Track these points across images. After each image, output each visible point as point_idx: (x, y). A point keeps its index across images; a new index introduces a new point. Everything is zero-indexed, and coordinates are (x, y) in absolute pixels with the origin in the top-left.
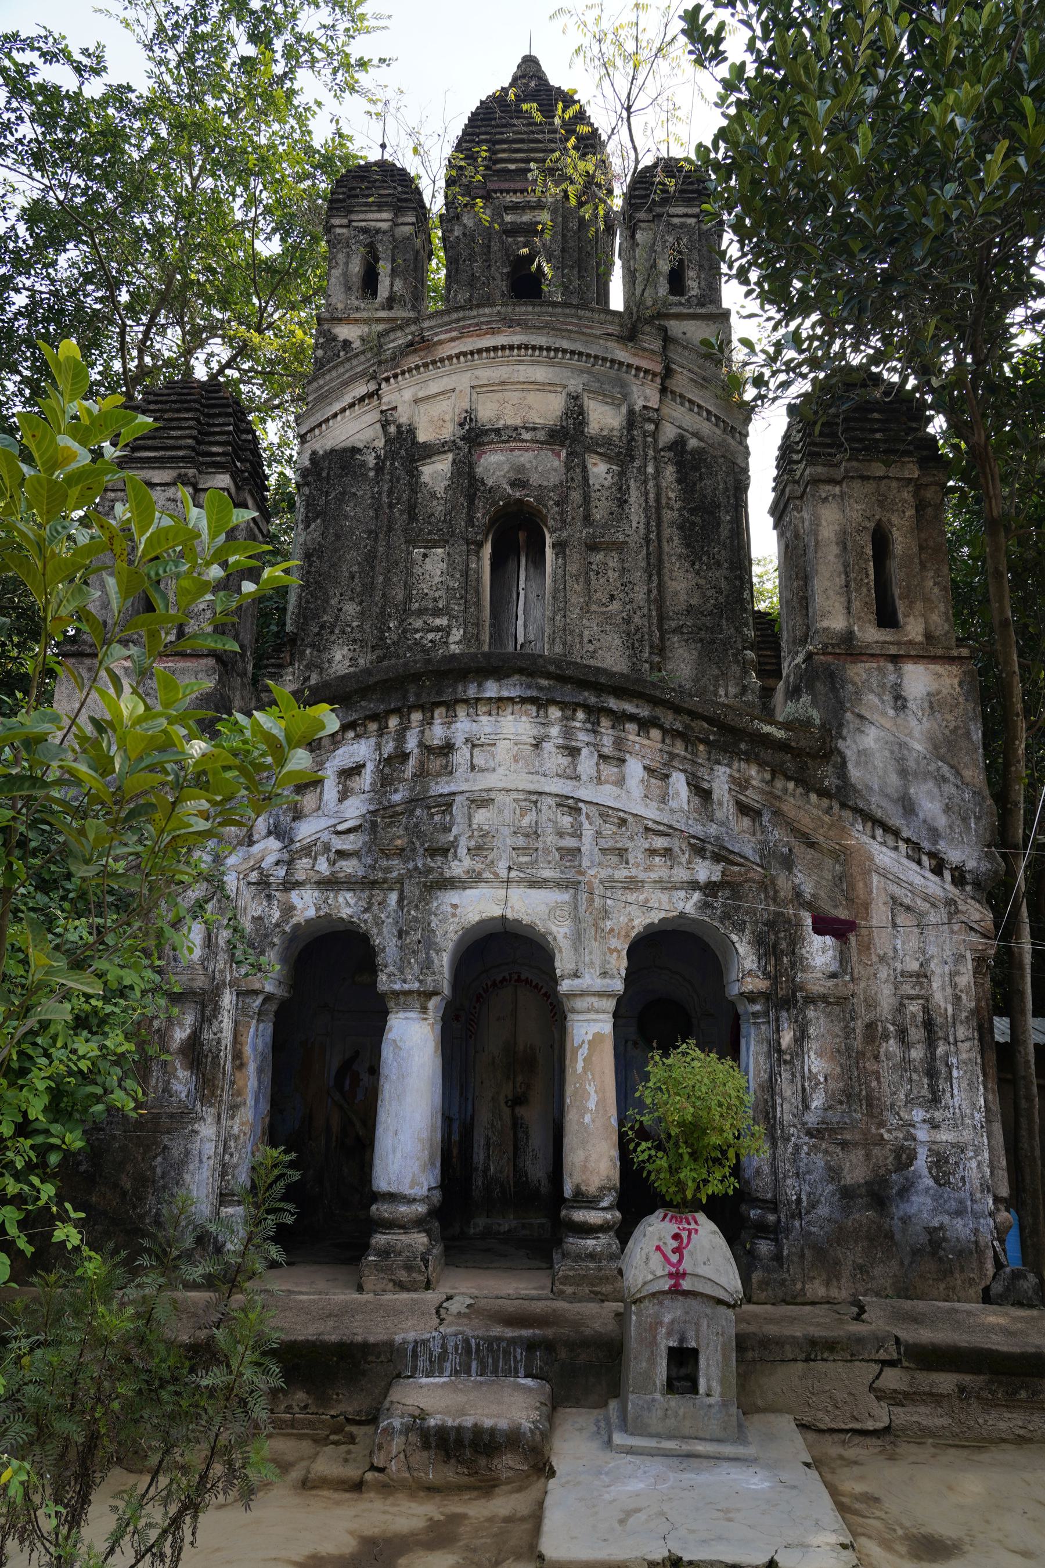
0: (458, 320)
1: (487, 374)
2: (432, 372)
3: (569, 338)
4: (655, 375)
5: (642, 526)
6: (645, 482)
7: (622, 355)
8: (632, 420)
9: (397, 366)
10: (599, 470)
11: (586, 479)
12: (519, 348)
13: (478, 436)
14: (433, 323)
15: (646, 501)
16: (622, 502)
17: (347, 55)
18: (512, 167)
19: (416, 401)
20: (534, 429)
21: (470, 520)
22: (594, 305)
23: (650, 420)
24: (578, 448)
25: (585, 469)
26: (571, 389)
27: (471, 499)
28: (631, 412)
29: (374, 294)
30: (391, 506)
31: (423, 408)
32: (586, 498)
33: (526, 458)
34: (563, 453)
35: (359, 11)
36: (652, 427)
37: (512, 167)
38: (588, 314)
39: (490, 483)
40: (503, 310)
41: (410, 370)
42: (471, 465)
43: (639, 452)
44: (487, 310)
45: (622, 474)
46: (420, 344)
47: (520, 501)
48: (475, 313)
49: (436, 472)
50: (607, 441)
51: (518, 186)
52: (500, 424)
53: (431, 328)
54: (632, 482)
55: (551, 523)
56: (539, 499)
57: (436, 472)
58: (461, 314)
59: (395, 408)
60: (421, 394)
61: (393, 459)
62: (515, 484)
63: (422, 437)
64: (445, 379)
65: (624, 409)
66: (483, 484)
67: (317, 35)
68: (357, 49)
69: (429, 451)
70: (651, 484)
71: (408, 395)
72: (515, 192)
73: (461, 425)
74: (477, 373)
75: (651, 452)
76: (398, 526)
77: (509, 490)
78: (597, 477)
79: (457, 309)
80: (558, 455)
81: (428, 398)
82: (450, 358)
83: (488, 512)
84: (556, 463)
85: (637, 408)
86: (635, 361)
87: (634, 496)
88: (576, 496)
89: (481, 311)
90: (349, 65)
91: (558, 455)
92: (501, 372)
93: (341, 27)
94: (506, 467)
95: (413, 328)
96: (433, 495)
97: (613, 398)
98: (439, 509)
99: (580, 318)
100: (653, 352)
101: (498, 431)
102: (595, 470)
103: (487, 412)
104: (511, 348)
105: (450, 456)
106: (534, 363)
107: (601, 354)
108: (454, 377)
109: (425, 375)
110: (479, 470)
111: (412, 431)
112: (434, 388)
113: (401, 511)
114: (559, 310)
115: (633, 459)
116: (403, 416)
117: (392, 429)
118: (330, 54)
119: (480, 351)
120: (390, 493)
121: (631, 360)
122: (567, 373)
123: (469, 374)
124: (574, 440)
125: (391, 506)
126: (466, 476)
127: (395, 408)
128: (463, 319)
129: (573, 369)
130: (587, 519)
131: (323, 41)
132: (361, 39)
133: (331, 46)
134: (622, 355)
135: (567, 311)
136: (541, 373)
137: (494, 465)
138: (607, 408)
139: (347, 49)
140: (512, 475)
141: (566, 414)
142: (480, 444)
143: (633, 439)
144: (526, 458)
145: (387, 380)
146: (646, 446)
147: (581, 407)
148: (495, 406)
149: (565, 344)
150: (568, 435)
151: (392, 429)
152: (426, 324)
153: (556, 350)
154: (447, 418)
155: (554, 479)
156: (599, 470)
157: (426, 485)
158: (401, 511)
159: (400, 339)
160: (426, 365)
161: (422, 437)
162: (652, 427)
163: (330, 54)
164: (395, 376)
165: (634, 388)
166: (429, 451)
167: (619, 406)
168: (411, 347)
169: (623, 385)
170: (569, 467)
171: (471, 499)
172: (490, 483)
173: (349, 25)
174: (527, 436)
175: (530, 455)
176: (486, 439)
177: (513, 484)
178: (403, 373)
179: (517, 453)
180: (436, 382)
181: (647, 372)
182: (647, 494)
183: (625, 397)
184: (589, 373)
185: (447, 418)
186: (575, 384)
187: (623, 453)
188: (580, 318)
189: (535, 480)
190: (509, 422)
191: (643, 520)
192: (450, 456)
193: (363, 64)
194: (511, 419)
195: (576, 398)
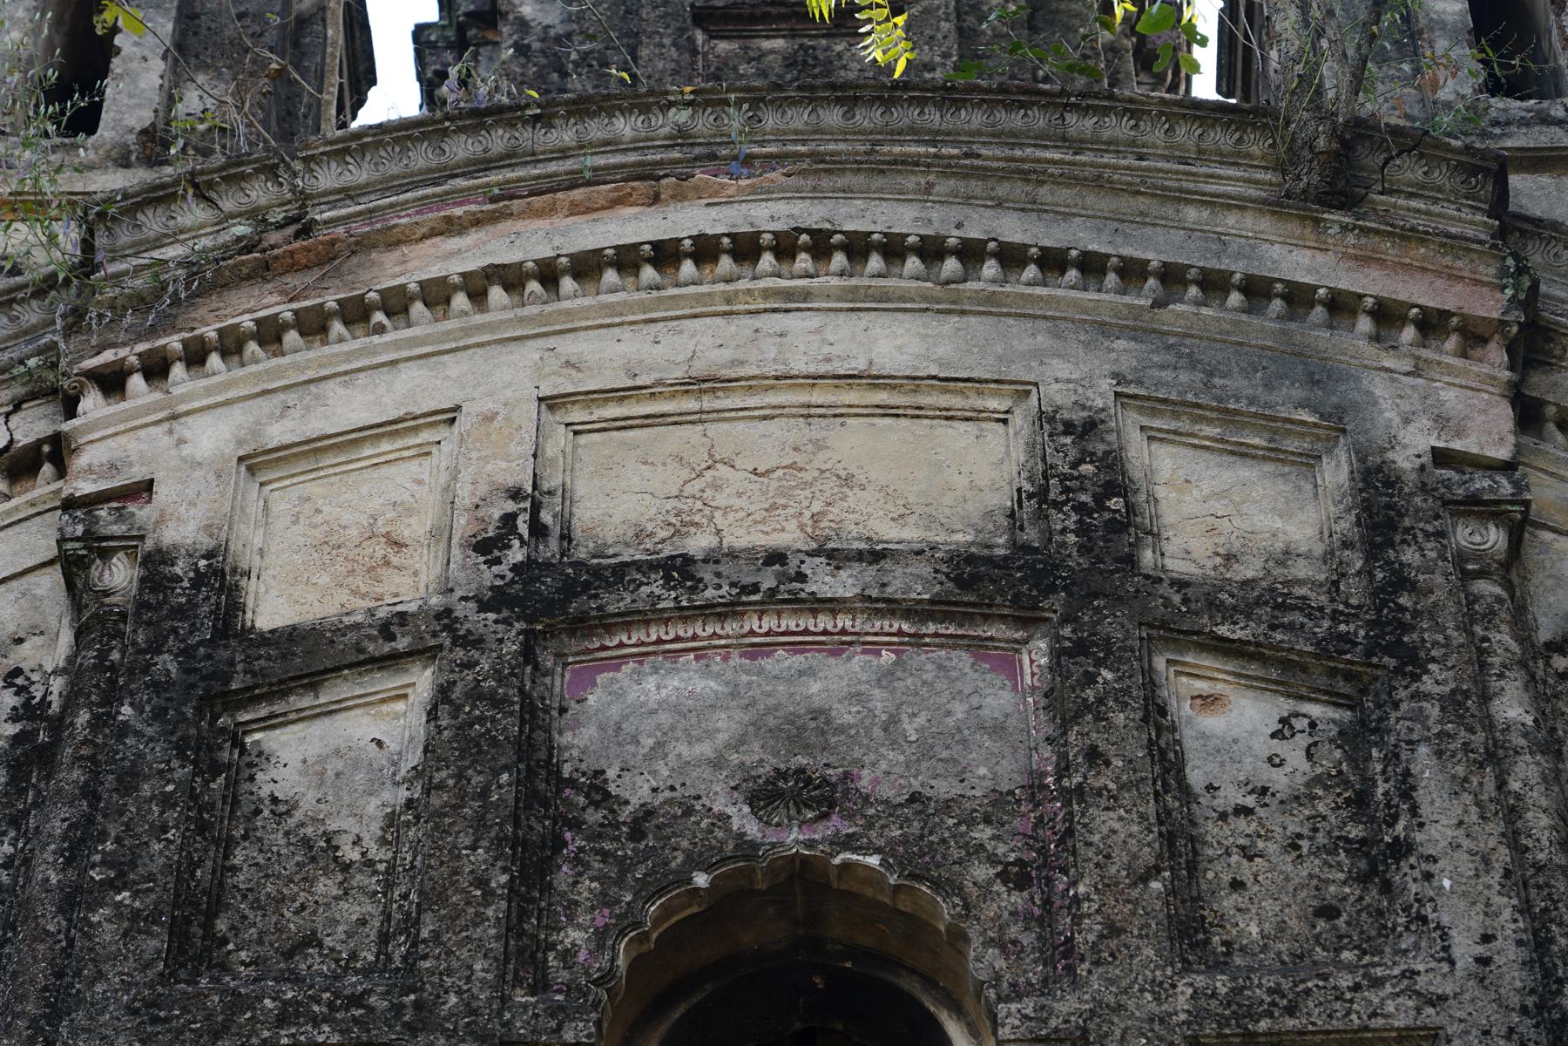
0: (485, 164)
1: (616, 345)
2: (344, 344)
3: (1031, 207)
4: (1473, 336)
5: (1508, 954)
6: (1495, 757)
7: (1295, 259)
8: (1381, 509)
9: (167, 324)
10: (1235, 727)
11: (1167, 761)
12: (785, 247)
13: (570, 589)
14: (359, 174)
15: (1513, 839)
16: (1380, 857)
19: (256, 462)
20: (875, 556)
21: (525, 957)
22: (1135, 88)
23: (1477, 508)
24: (1114, 626)
25: (1155, 712)
26: (1056, 394)
27: (533, 868)
28: (1375, 483)
29: (86, 121)
30: (74, 899)
31: (287, 496)
32: (1179, 845)
33: (832, 682)
34: (1036, 656)
36: (1494, 538)
38: (1117, 128)
39: (637, 791)
40: (703, 124)
41: (231, 345)
42: (537, 718)
43: (1441, 633)
44: (625, 127)
45: (1355, 739)
46: (291, 247)
47: (803, 874)
48: (565, 135)
49: (341, 759)
50: (1272, 599)
52: (698, 543)
53: (347, 194)
54: (1423, 761)
55: (984, 961)
56: (917, 861)
57: (341, 759)
58: (498, 140)
59: (146, 488)
60: (279, 433)
61: (111, 697)
62: (766, 795)
63: (272, 607)
64: (411, 375)
65: (1336, 472)
66: (598, 791)
69: (309, 662)
70: (1526, 771)
71: (212, 437)
73: (487, 548)
74: (569, 346)
75: (1503, 639)
76: (109, 989)
77: (753, 829)
78: (1226, 750)
79: (479, 118)
80: (1010, 668)
81: (314, 449)
82: (436, 294)
83: (628, 922)
84: (999, 700)
85: (1404, 461)
86: (1371, 283)
87: (1443, 820)
88: (1119, 828)
89: (595, 129)
91: (1010, 668)
92: (704, 343)
94: (726, 724)
95: (259, 193)
96: (321, 852)
97: (1271, 423)
98: (347, 916)
99: (1078, 145)
100: (1455, 244)
101: (680, 570)
102: (1212, 723)
103: (619, 499)
104: (746, 248)
105: (422, 681)
106: (856, 303)
107: (1194, 257)
108: (454, 367)
109: (299, 356)
110: (579, 741)
111: (220, 579)
112: (349, 407)
113: (134, 923)
114: (975, 119)
115: (1412, 663)
116: (180, 521)
117: (120, 575)
119: (587, 267)
120: (75, 850)
121: (1348, 280)
122: (1024, 338)
123: (531, 353)
124: (1084, 592)
125: (74, 899)
126: (509, 778)
127: (146, 488)
128: (509, 158)
129: (1054, 320)
130: (1190, 934)
134: (1295, 259)
135: (1015, 120)
136: (895, 343)
137: (660, 721)
138: (1246, 472)
140: (761, 758)
141: (1040, 495)
142: (583, 625)
143: (1400, 581)
144: (832, 682)
145: (112, 382)
146: (1472, 612)
147: (1113, 462)
148: (670, 478)
149: (1013, 229)
150: (1061, 573)
151: (120, 575)
152: (327, 178)
153: (972, 253)
154: (415, 529)
155: (991, 768)
156: (1235, 727)
157: (282, 808)
158: (134, 923)
159: (194, 229)
160: (314, 326)
161: (272, 607)
162: (1494, 538)
164: (156, 369)
165: (1380, 388)
166: (309, 662)
167: (1309, 461)
168: (250, 264)
169: (1319, 376)
170: (1065, 705)
171: (533, 868)
172: (637, 791)
174: (843, 584)
175: (858, 662)
176: (615, 602)
177: (766, 795)
178: (195, 357)
179: (784, 661)
180: (355, 387)
181: (1432, 324)
182: (1512, 812)
183: (1336, 423)
184: (1139, 332)
185: (415, 529)
186: (1074, 376)
187: (1352, 645)
188: (1078, 145)
189: (883, 774)
190: (740, 537)
191: (1508, 923)
192: (422, 681)
194: (743, 519)
195: (1088, 429)
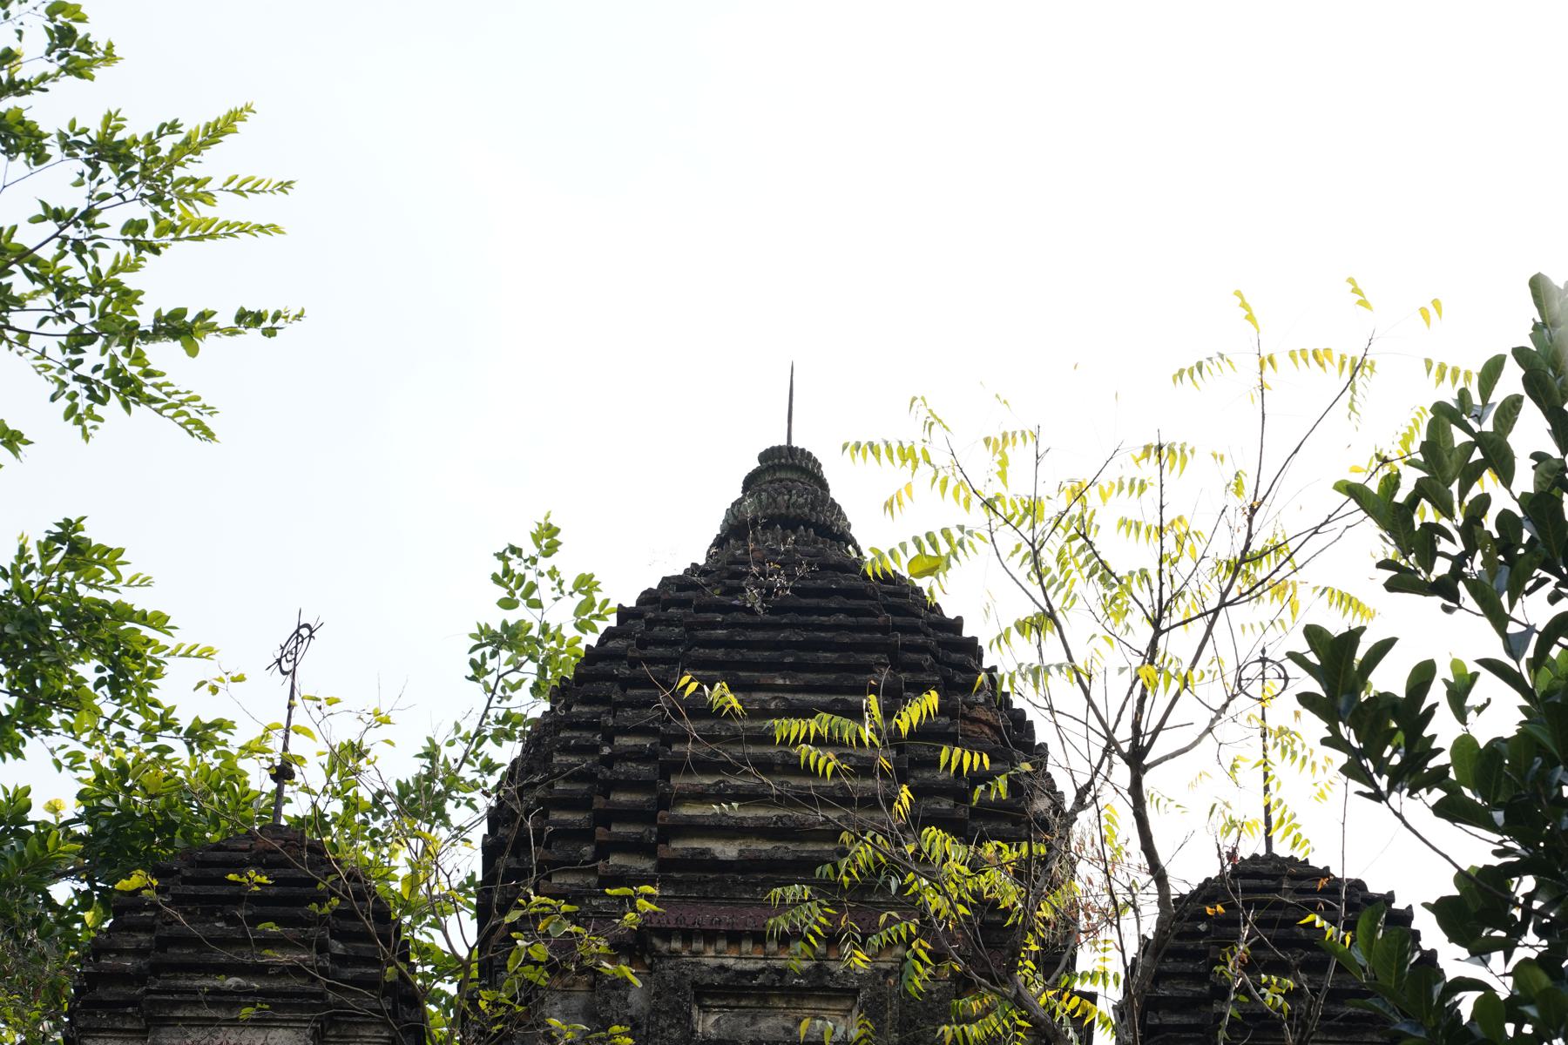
17: (128, 297)
18: (727, 850)
35: (178, 173)
37: (727, 850)
51: (745, 919)
67: (27, 237)
68: (161, 285)
72: (735, 938)
90: (130, 334)
93: (114, 217)
118: (67, 292)
131: (47, 253)
132: (178, 252)
133: (73, 268)
139: (129, 280)
163: (67, 292)
173: (142, 212)
193: (176, 327)
